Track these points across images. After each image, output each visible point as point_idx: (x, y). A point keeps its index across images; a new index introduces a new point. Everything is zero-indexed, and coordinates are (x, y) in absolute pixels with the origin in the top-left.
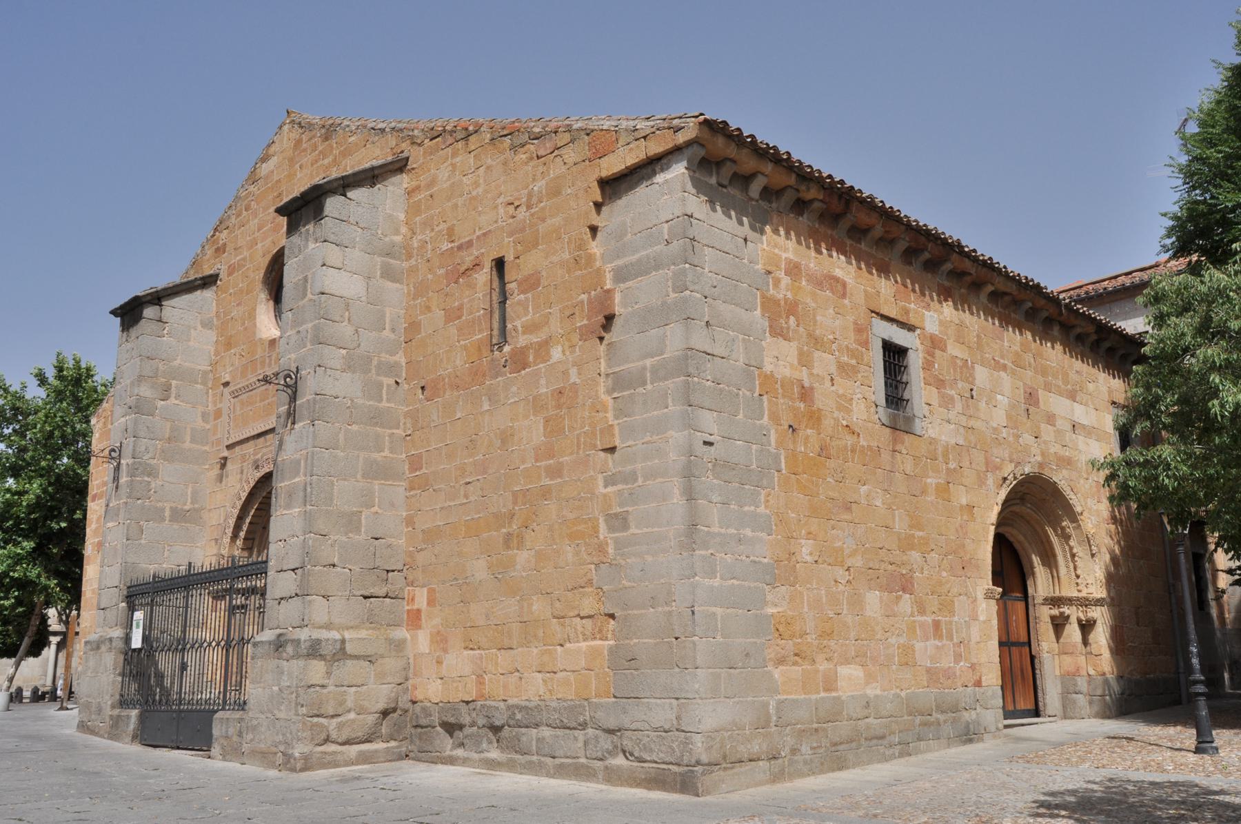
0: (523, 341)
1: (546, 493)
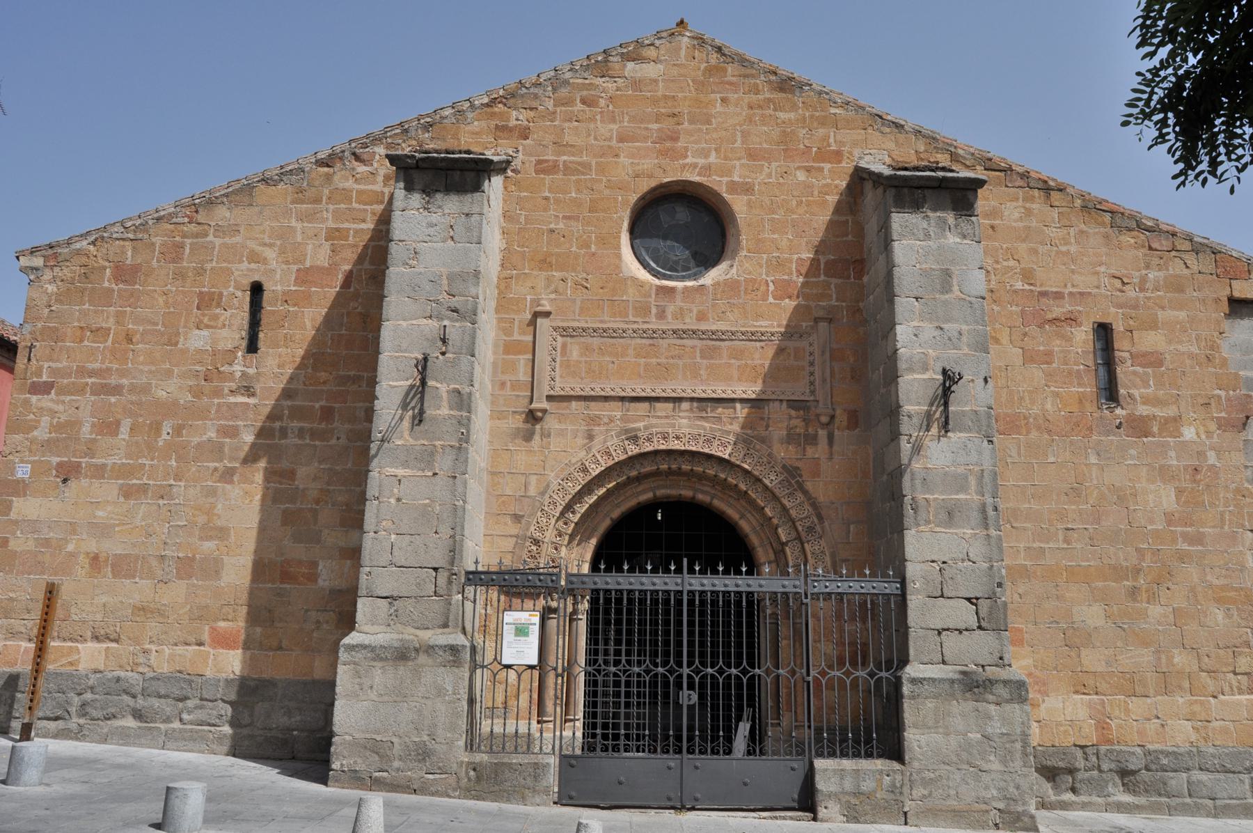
0: (1143, 410)
1: (1182, 557)
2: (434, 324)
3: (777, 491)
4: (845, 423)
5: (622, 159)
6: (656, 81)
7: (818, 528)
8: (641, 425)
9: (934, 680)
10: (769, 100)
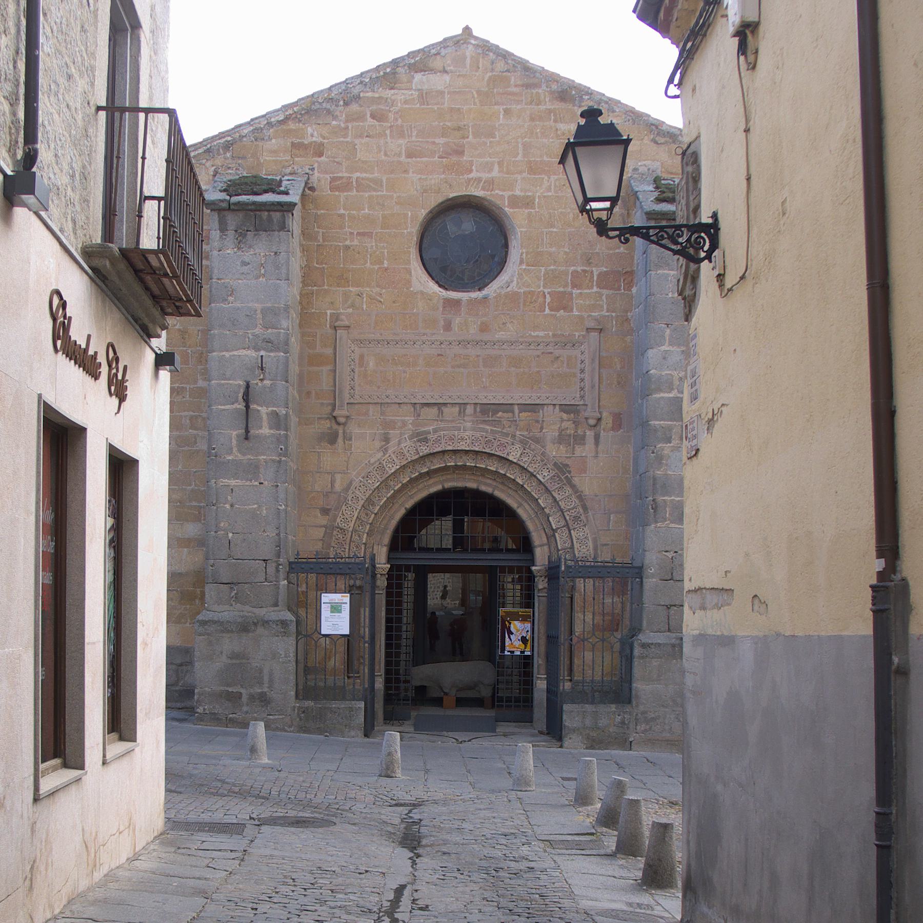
2: (251, 353)
4: (610, 425)
5: (411, 174)
6: (442, 93)
7: (583, 517)
9: (659, 645)
10: (550, 111)
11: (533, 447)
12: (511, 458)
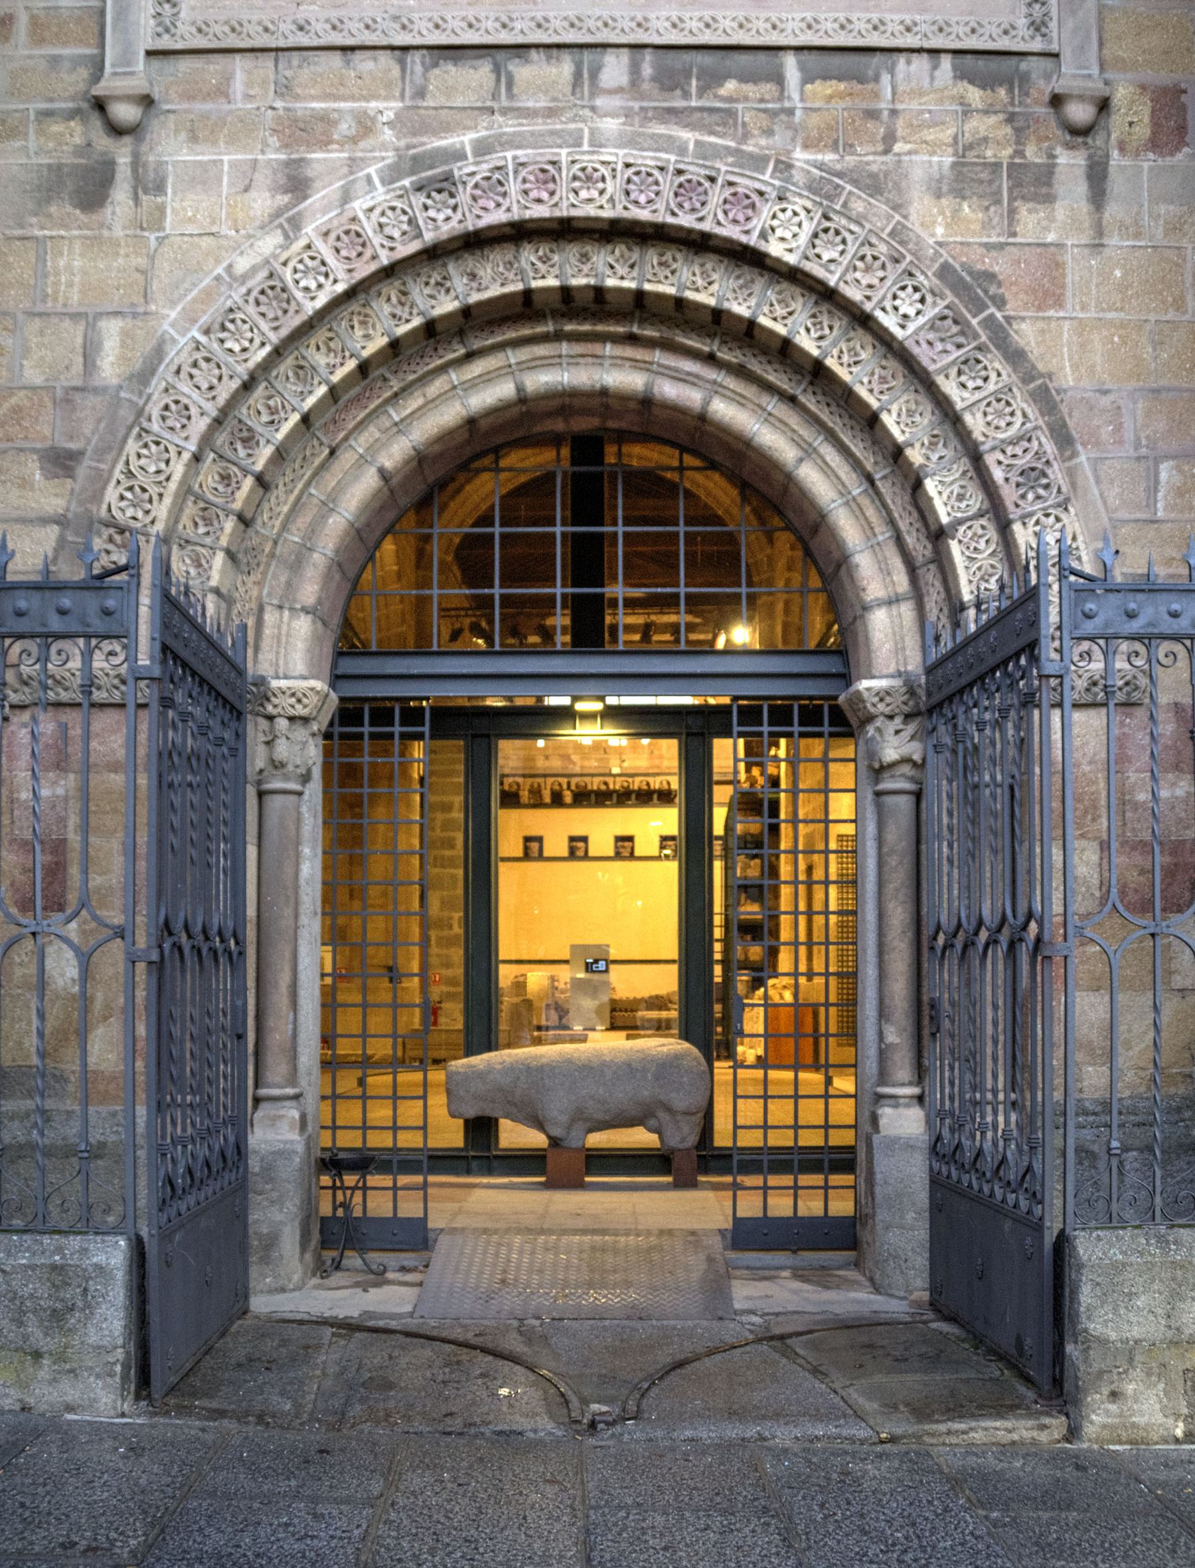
3: (923, 354)
4: (1143, 131)
7: (1056, 474)
8: (465, 139)
11: (858, 207)
12: (775, 249)
